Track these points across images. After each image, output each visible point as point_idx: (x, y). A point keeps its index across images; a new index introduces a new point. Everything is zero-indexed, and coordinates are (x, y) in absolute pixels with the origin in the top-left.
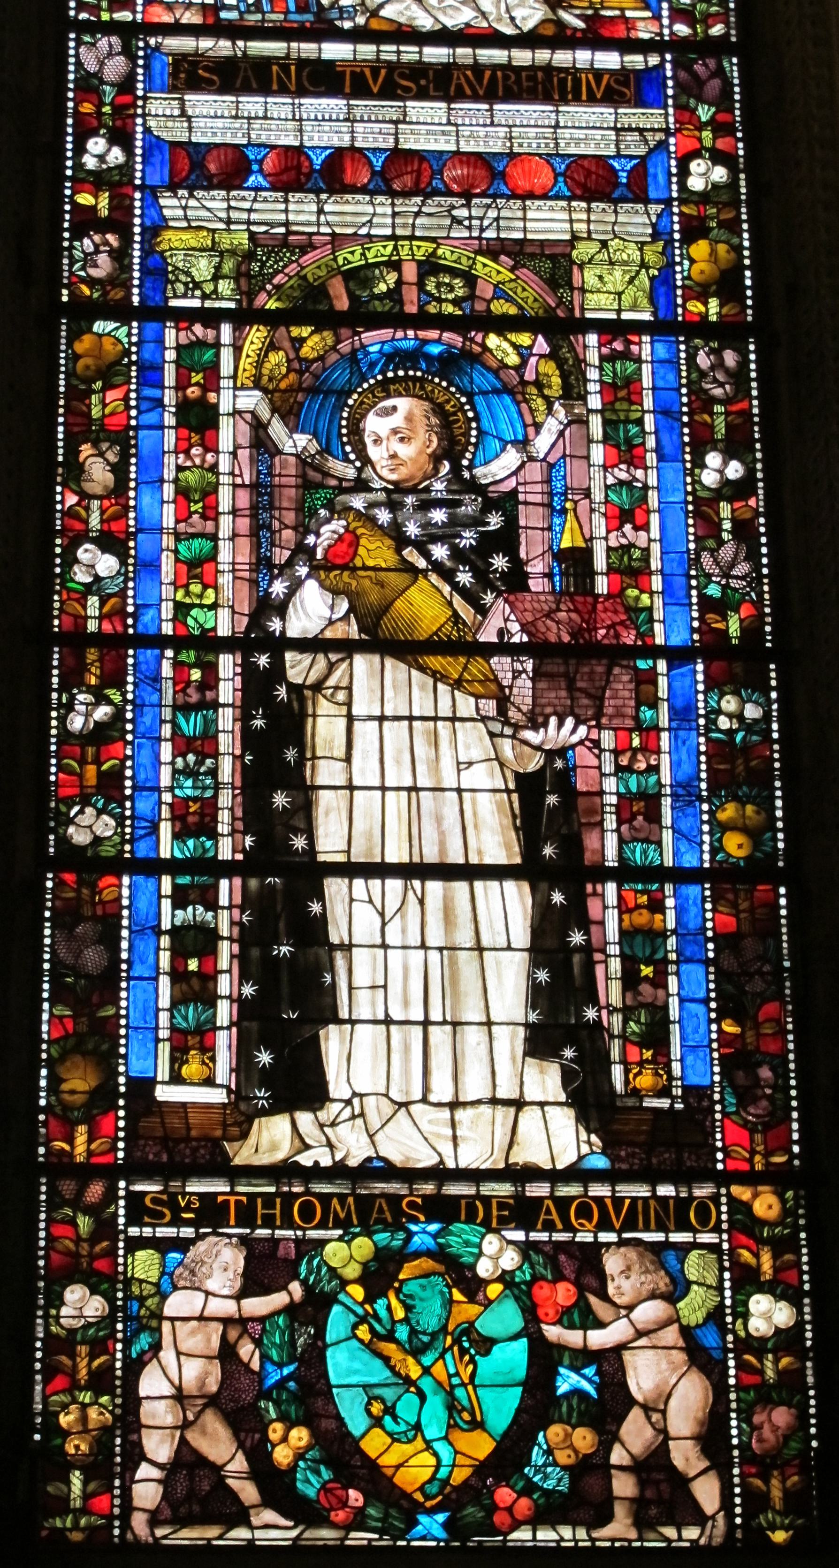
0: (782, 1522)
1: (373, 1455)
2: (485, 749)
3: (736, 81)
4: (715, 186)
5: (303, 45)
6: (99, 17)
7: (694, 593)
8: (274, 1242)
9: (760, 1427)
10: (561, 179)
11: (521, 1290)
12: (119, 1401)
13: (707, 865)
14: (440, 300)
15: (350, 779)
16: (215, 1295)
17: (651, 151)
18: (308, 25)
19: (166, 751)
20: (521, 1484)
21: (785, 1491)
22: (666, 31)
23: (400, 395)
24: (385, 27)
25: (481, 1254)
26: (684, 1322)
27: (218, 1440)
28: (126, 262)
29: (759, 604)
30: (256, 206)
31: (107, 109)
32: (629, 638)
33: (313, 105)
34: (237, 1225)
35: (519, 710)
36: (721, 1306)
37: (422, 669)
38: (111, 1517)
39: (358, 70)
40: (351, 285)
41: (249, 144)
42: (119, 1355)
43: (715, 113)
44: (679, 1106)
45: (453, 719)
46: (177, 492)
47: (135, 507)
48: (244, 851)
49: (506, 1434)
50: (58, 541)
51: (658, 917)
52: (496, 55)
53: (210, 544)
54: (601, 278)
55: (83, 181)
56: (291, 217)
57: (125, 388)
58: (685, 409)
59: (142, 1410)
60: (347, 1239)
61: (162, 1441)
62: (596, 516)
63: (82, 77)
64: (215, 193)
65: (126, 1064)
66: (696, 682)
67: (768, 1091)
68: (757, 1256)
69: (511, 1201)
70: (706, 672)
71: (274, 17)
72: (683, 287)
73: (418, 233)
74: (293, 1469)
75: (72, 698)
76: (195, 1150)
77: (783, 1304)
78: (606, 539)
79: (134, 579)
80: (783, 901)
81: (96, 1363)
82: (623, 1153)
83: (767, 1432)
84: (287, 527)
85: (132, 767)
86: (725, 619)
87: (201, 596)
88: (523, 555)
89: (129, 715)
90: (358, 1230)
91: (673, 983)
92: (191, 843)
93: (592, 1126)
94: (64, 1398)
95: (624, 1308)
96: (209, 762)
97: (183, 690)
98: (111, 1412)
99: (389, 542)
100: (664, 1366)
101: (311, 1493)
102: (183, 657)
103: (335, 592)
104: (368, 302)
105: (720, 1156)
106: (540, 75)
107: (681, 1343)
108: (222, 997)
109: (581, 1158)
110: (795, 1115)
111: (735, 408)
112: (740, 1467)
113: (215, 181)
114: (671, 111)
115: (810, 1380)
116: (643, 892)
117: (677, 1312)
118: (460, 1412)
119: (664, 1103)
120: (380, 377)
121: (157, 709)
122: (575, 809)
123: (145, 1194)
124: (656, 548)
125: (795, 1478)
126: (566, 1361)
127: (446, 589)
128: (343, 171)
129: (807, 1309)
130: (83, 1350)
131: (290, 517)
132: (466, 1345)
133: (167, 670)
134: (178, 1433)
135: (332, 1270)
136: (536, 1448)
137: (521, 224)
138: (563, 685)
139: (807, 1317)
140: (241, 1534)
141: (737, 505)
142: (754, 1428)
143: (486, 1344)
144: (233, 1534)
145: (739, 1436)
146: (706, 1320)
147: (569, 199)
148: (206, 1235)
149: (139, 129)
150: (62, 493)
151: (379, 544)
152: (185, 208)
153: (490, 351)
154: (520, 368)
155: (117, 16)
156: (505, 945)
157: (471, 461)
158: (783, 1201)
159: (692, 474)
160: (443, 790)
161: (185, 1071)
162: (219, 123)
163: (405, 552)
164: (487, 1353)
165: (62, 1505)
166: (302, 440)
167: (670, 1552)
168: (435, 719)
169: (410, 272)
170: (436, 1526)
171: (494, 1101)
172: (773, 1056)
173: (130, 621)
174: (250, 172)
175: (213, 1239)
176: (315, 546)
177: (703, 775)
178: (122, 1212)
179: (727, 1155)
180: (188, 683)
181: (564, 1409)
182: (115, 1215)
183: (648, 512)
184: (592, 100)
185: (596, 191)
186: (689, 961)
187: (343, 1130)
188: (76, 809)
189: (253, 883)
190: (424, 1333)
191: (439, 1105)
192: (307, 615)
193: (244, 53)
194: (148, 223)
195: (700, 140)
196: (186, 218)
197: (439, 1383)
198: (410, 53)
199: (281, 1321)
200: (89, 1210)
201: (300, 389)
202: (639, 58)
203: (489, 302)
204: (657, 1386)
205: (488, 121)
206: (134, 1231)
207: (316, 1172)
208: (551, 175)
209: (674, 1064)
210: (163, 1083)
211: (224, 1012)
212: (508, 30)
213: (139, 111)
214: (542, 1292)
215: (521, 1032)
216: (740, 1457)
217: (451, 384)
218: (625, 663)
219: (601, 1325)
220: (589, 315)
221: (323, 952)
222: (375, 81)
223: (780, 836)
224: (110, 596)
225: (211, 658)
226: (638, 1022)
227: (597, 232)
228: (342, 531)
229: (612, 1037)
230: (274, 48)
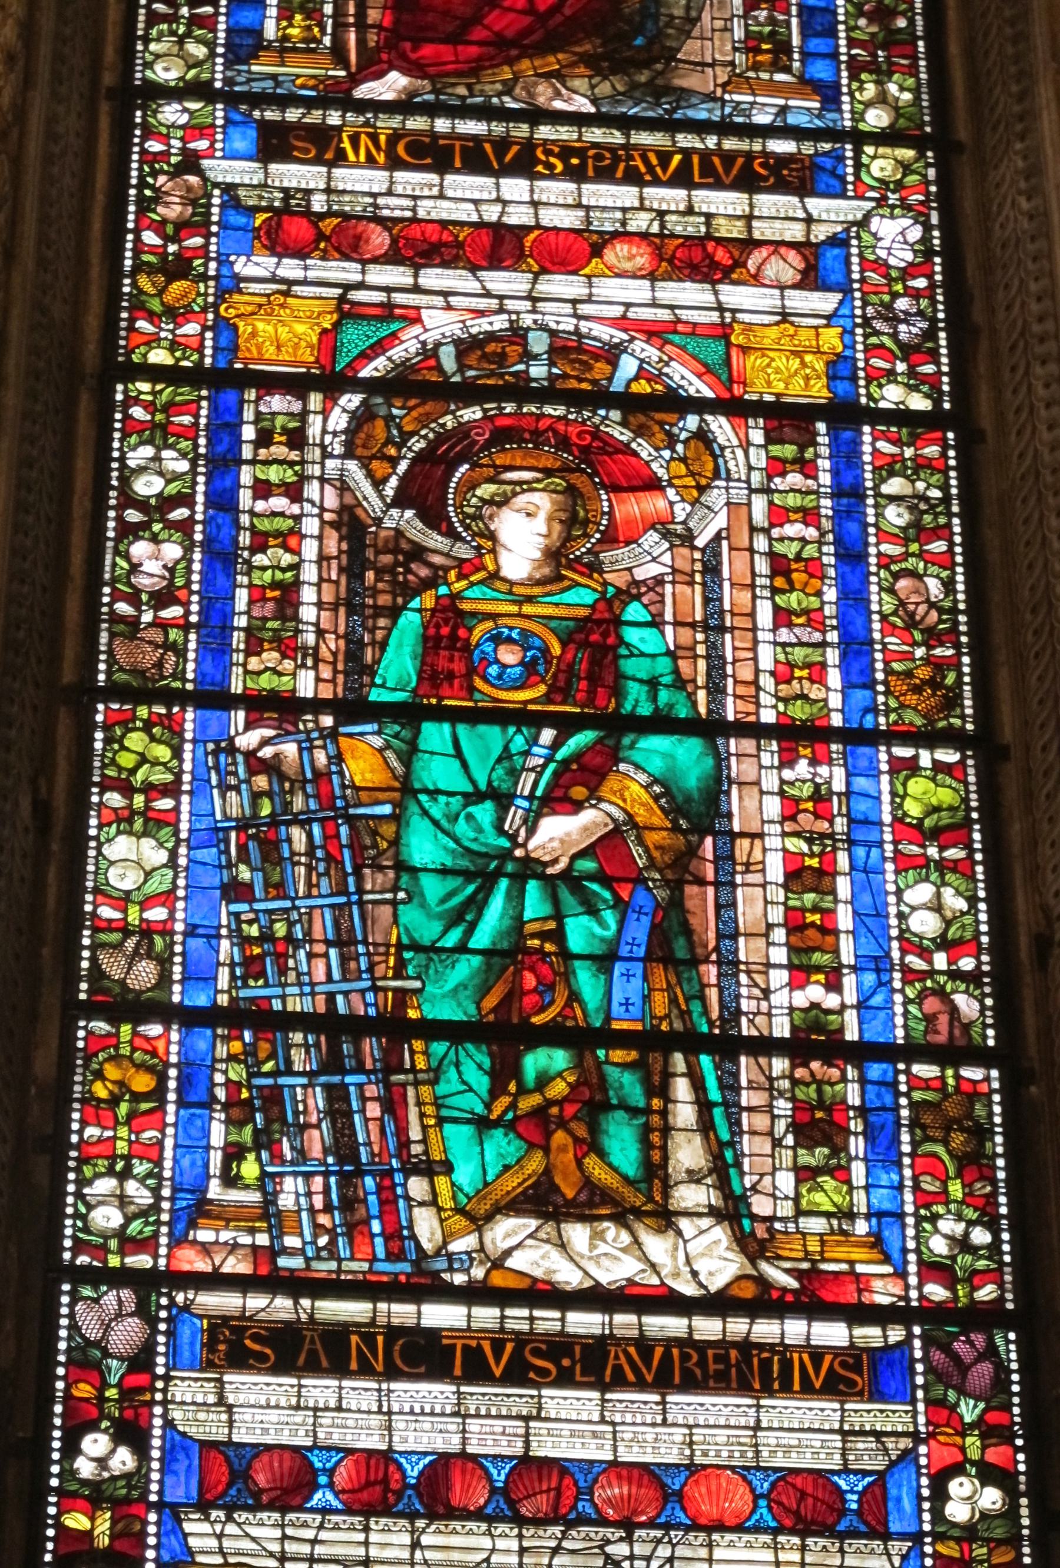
3: (1014, 1366)
4: (984, 1516)
5: (396, 1307)
6: (105, 1261)
10: (763, 1503)
17: (892, 1464)
18: (403, 1278)
22: (914, 1294)
24: (512, 1283)
30: (323, 1535)
31: (112, 1393)
39: (474, 1343)
41: (315, 1447)
43: (984, 1411)
52: (673, 1325)
56: (374, 1552)
63: (78, 1347)
64: (264, 1515)
71: (354, 1266)
106: (733, 1353)
113: (265, 1498)
114: (921, 1407)
147: (776, 1532)
149: (157, 1422)
152: (220, 1537)
155: (129, 1260)
162: (273, 1416)
174: (316, 1487)
184: (808, 1390)
185: (813, 1522)
193: (311, 1316)
194: (166, 1557)
195: (963, 1449)
196: (221, 1551)
198: (548, 1320)
202: (875, 1331)
205: (659, 1419)
208: (749, 1497)
212: (688, 1289)
213: (159, 1396)
222: (498, 1361)
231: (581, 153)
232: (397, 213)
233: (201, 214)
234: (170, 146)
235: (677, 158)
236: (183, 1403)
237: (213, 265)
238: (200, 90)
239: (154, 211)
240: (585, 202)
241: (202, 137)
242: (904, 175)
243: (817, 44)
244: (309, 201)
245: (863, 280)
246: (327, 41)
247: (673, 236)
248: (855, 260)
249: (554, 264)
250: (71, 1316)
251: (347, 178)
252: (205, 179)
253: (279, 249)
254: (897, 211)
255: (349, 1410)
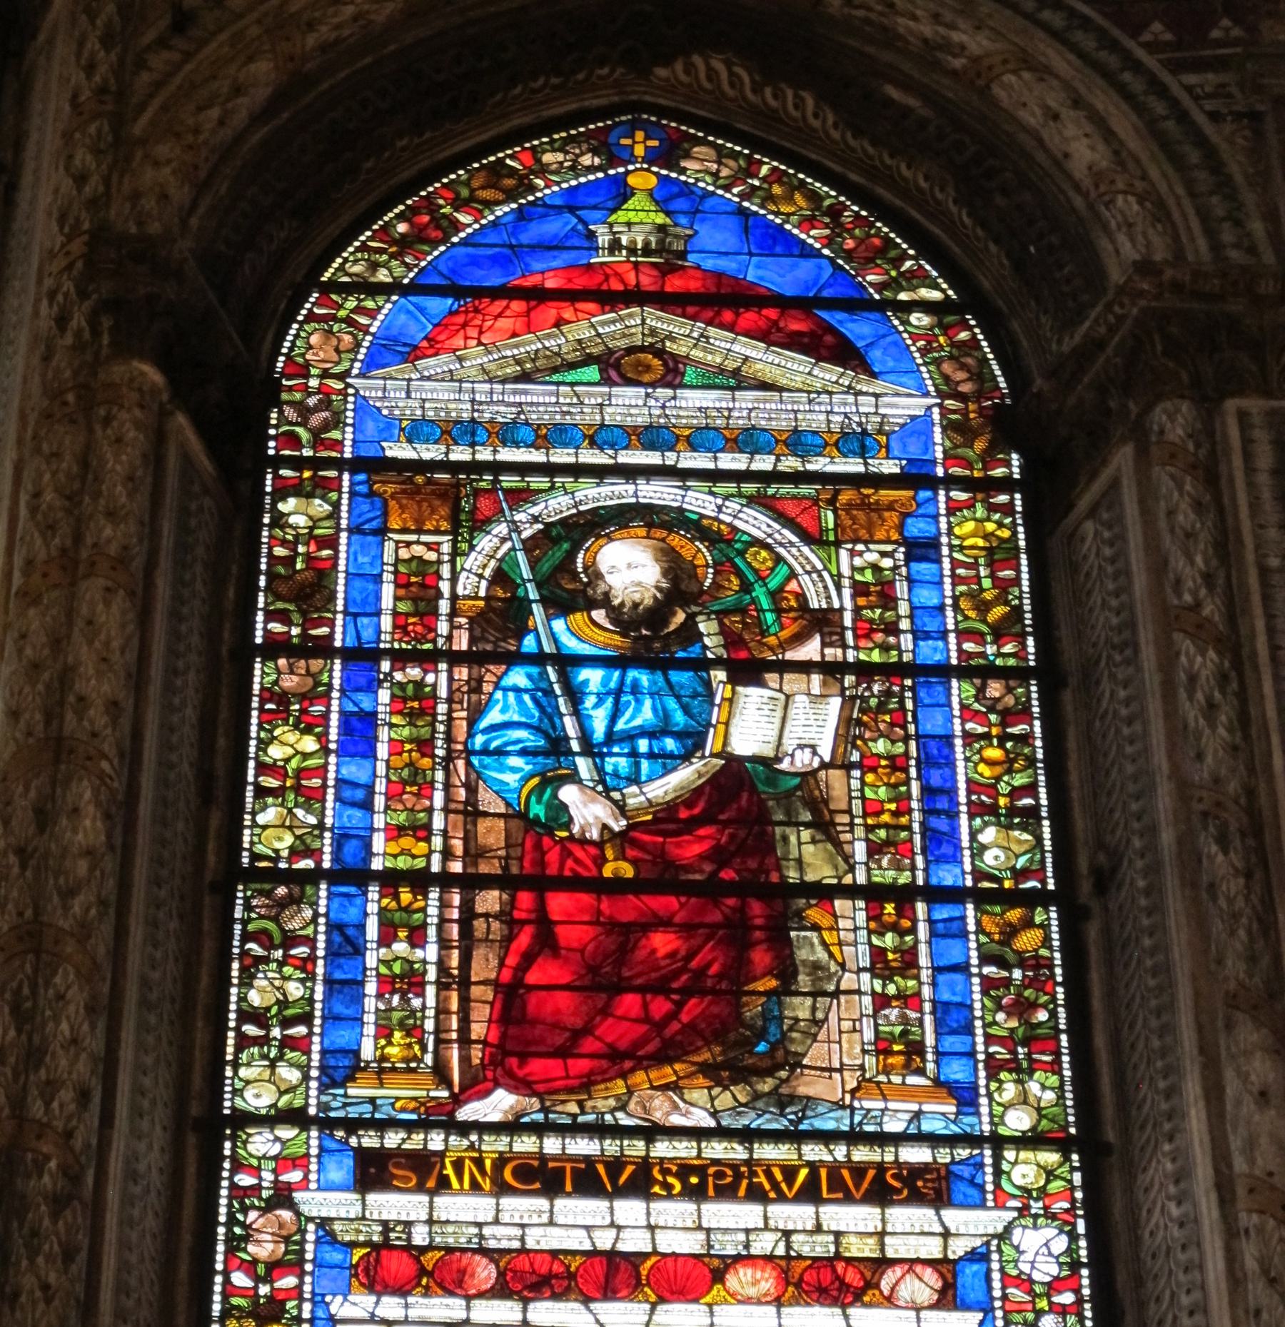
231: (701, 1170)
232: (505, 1244)
233: (294, 1252)
234: (260, 1178)
235: (804, 1173)
237: (307, 1307)
238: (296, 1117)
239: (245, 1250)
240: (705, 1225)
241: (295, 1167)
242: (1048, 1181)
243: (953, 1043)
244: (409, 1234)
245: (1005, 1298)
246: (429, 1059)
247: (800, 1257)
248: (996, 1276)
249: (672, 1293)
251: (448, 1206)
252: (298, 1214)
253: (378, 1288)
254: (1041, 1221)
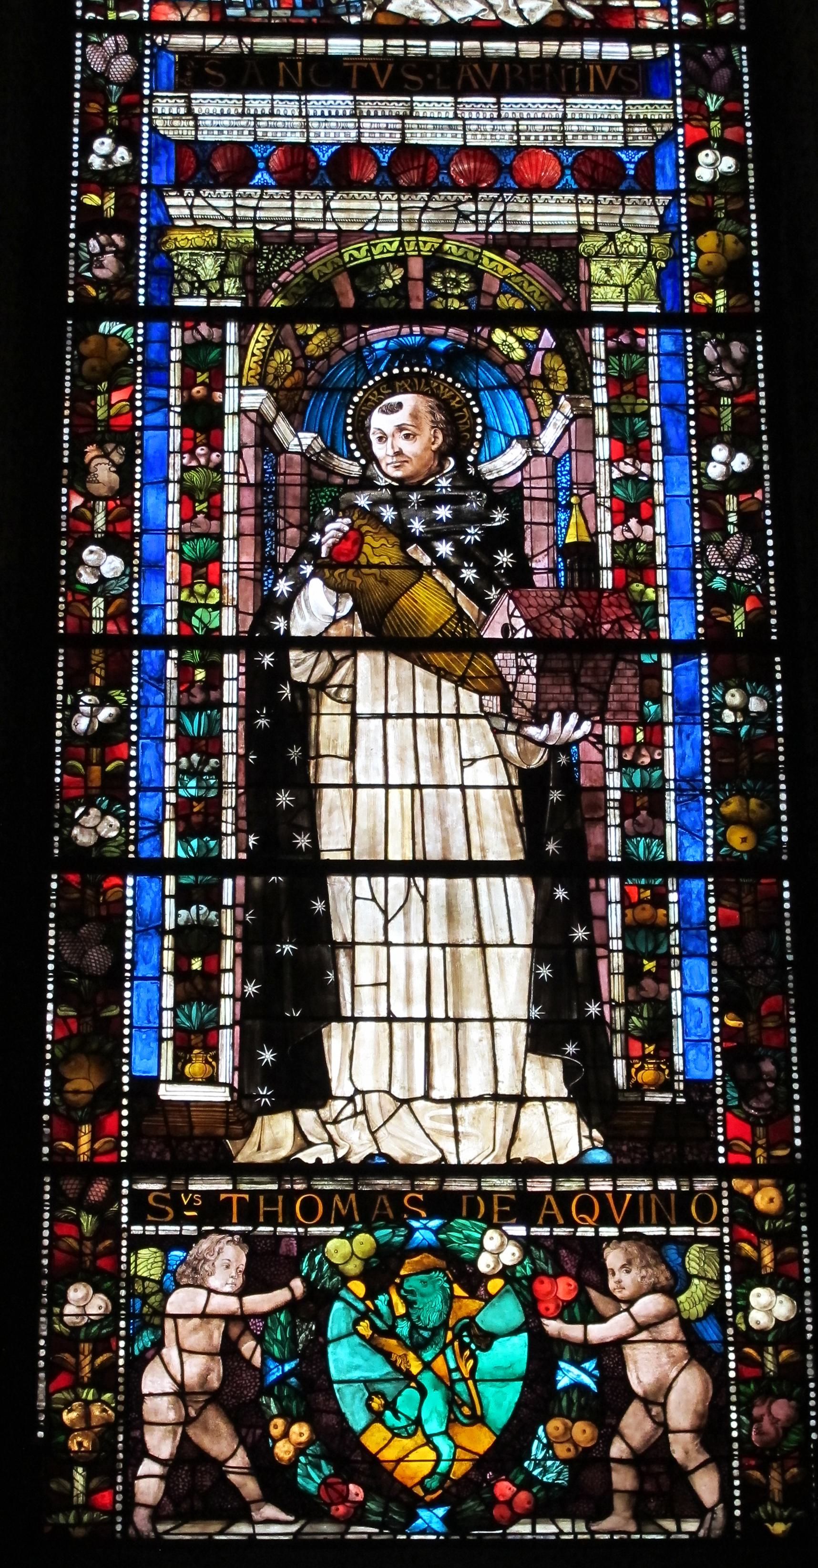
0: (781, 1515)
1: (373, 1449)
2: (488, 745)
3: (745, 70)
4: (723, 175)
5: (310, 41)
6: (106, 16)
7: (699, 586)
8: (276, 1239)
9: (759, 1420)
10: (568, 172)
11: (521, 1285)
12: (121, 1398)
13: (710, 859)
14: (446, 296)
15: (354, 777)
16: (217, 1292)
17: (659, 142)
19: (170, 752)
20: (521, 1477)
21: (784, 1482)
22: (675, 21)
23: (406, 392)
24: (391, 21)
25: (482, 1249)
26: (685, 1315)
27: (220, 1435)
28: (132, 262)
29: (764, 597)
30: (263, 204)
31: (113, 109)
32: (634, 633)
33: (317, 101)
34: (239, 1223)
35: (523, 706)
36: (722, 1298)
37: (426, 666)
38: (113, 1513)
40: (358, 282)
41: (256, 141)
42: (122, 1353)
43: (723, 103)
44: (681, 1100)
45: (457, 716)
46: (182, 493)
47: (140, 508)
48: (247, 850)
49: (507, 1428)
50: (64, 543)
51: (662, 912)
52: (505, 48)
53: (214, 544)
54: (607, 271)
55: (89, 181)
56: (297, 214)
57: (130, 389)
58: (691, 402)
59: (145, 1407)
60: (349, 1235)
61: (164, 1438)
62: (601, 511)
64: (221, 191)
65: (129, 1064)
66: (701, 676)
67: (770, 1085)
68: (758, 1249)
69: (513, 1197)
70: (709, 666)
71: (280, 13)
72: (690, 279)
73: (424, 229)
74: (294, 1463)
75: (77, 699)
76: (198, 1148)
77: (783, 1298)
78: (611, 533)
79: (138, 580)
80: (786, 895)
81: (99, 1361)
82: (624, 1148)
83: (766, 1424)
84: (292, 526)
85: (136, 768)
86: (730, 612)
87: (205, 596)
88: (528, 550)
89: (134, 716)
90: (359, 1226)
91: (675, 978)
92: (194, 843)
93: (594, 1122)
94: (66, 1395)
95: (624, 1302)
96: (213, 761)
97: (188, 690)
98: (113, 1409)
99: (393, 539)
100: (664, 1359)
101: (312, 1488)
102: (187, 657)
103: (340, 590)
104: (374, 298)
105: (721, 1150)
106: (548, 67)
107: (681, 1337)
108: (225, 996)
109: (582, 1153)
110: (797, 1108)
111: (741, 400)
112: (739, 1460)
114: (679, 101)
115: (810, 1372)
116: (646, 887)
117: (677, 1305)
118: (460, 1407)
119: (666, 1098)
120: (385, 374)
121: (161, 710)
122: (578, 803)
123: (150, 1192)
124: (661, 542)
125: (795, 1470)
126: (567, 1355)
127: (451, 586)
128: (349, 167)
129: (807, 1302)
130: (86, 1347)
131: (295, 516)
132: (467, 1340)
133: (171, 670)
134: (180, 1430)
135: (334, 1267)
136: (536, 1442)
137: (527, 218)
138: (567, 680)
139: (808, 1310)
140: (243, 1529)
141: (743, 498)
142: (754, 1420)
143: (486, 1339)
144: (235, 1529)
145: (738, 1429)
146: (707, 1313)
147: (576, 192)
148: (209, 1232)
149: (145, 128)
150: (67, 495)
151: (383, 541)
152: (191, 207)
153: (496, 346)
154: (526, 363)
156: (507, 942)
157: (476, 457)
158: (784, 1194)
159: (698, 468)
160: (447, 787)
161: (188, 1070)
162: (226, 121)
163: (410, 550)
164: (487, 1347)
165: (65, 1500)
166: (307, 438)
167: (670, 1544)
168: (439, 716)
169: (416, 268)
170: (435, 1520)
171: (496, 1097)
172: (776, 1049)
173: (135, 622)
174: (256, 170)
175: (215, 1237)
176: (320, 544)
177: (708, 769)
178: (125, 1210)
179: (728, 1149)
180: (193, 682)
181: (564, 1403)
182: (119, 1214)
183: (654, 506)
184: (600, 92)
186: (691, 955)
187: (345, 1127)
188: (81, 810)
189: (257, 881)
190: (425, 1328)
191: (441, 1101)
192: (311, 614)
193: (251, 49)
194: (154, 223)
195: (708, 130)
196: (192, 217)
197: (439, 1377)
198: (417, 47)
199: (282, 1318)
200: (91, 1209)
201: (305, 387)
202: (647, 48)
203: (495, 296)
204: (658, 1380)
205: (495, 115)
206: (137, 1229)
207: (319, 1169)
208: (558, 168)
209: (676, 1058)
210: (166, 1082)
211: (227, 1011)
212: (515, 22)
213: (146, 110)
214: (543, 1287)
215: (523, 1028)
216: (739, 1450)
217: (456, 380)
218: (629, 657)
219: (602, 1319)
220: (596, 308)
221: (326, 951)
222: (382, 76)
223: (784, 829)
224: (115, 597)
225: (215, 658)
226: (640, 1017)
227: (604, 225)
228: (346, 528)
229: (614, 1032)
230: (281, 44)
236: (163, 114)
250: (83, 56)
255: (279, 116)
